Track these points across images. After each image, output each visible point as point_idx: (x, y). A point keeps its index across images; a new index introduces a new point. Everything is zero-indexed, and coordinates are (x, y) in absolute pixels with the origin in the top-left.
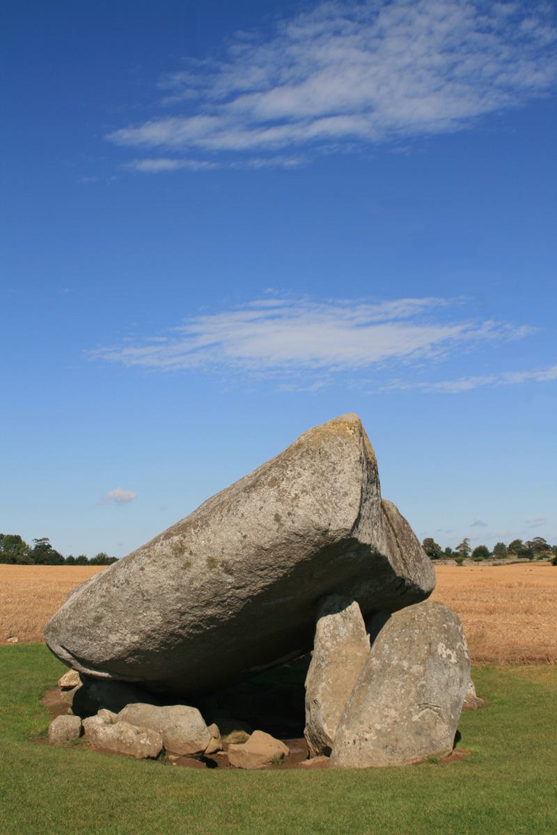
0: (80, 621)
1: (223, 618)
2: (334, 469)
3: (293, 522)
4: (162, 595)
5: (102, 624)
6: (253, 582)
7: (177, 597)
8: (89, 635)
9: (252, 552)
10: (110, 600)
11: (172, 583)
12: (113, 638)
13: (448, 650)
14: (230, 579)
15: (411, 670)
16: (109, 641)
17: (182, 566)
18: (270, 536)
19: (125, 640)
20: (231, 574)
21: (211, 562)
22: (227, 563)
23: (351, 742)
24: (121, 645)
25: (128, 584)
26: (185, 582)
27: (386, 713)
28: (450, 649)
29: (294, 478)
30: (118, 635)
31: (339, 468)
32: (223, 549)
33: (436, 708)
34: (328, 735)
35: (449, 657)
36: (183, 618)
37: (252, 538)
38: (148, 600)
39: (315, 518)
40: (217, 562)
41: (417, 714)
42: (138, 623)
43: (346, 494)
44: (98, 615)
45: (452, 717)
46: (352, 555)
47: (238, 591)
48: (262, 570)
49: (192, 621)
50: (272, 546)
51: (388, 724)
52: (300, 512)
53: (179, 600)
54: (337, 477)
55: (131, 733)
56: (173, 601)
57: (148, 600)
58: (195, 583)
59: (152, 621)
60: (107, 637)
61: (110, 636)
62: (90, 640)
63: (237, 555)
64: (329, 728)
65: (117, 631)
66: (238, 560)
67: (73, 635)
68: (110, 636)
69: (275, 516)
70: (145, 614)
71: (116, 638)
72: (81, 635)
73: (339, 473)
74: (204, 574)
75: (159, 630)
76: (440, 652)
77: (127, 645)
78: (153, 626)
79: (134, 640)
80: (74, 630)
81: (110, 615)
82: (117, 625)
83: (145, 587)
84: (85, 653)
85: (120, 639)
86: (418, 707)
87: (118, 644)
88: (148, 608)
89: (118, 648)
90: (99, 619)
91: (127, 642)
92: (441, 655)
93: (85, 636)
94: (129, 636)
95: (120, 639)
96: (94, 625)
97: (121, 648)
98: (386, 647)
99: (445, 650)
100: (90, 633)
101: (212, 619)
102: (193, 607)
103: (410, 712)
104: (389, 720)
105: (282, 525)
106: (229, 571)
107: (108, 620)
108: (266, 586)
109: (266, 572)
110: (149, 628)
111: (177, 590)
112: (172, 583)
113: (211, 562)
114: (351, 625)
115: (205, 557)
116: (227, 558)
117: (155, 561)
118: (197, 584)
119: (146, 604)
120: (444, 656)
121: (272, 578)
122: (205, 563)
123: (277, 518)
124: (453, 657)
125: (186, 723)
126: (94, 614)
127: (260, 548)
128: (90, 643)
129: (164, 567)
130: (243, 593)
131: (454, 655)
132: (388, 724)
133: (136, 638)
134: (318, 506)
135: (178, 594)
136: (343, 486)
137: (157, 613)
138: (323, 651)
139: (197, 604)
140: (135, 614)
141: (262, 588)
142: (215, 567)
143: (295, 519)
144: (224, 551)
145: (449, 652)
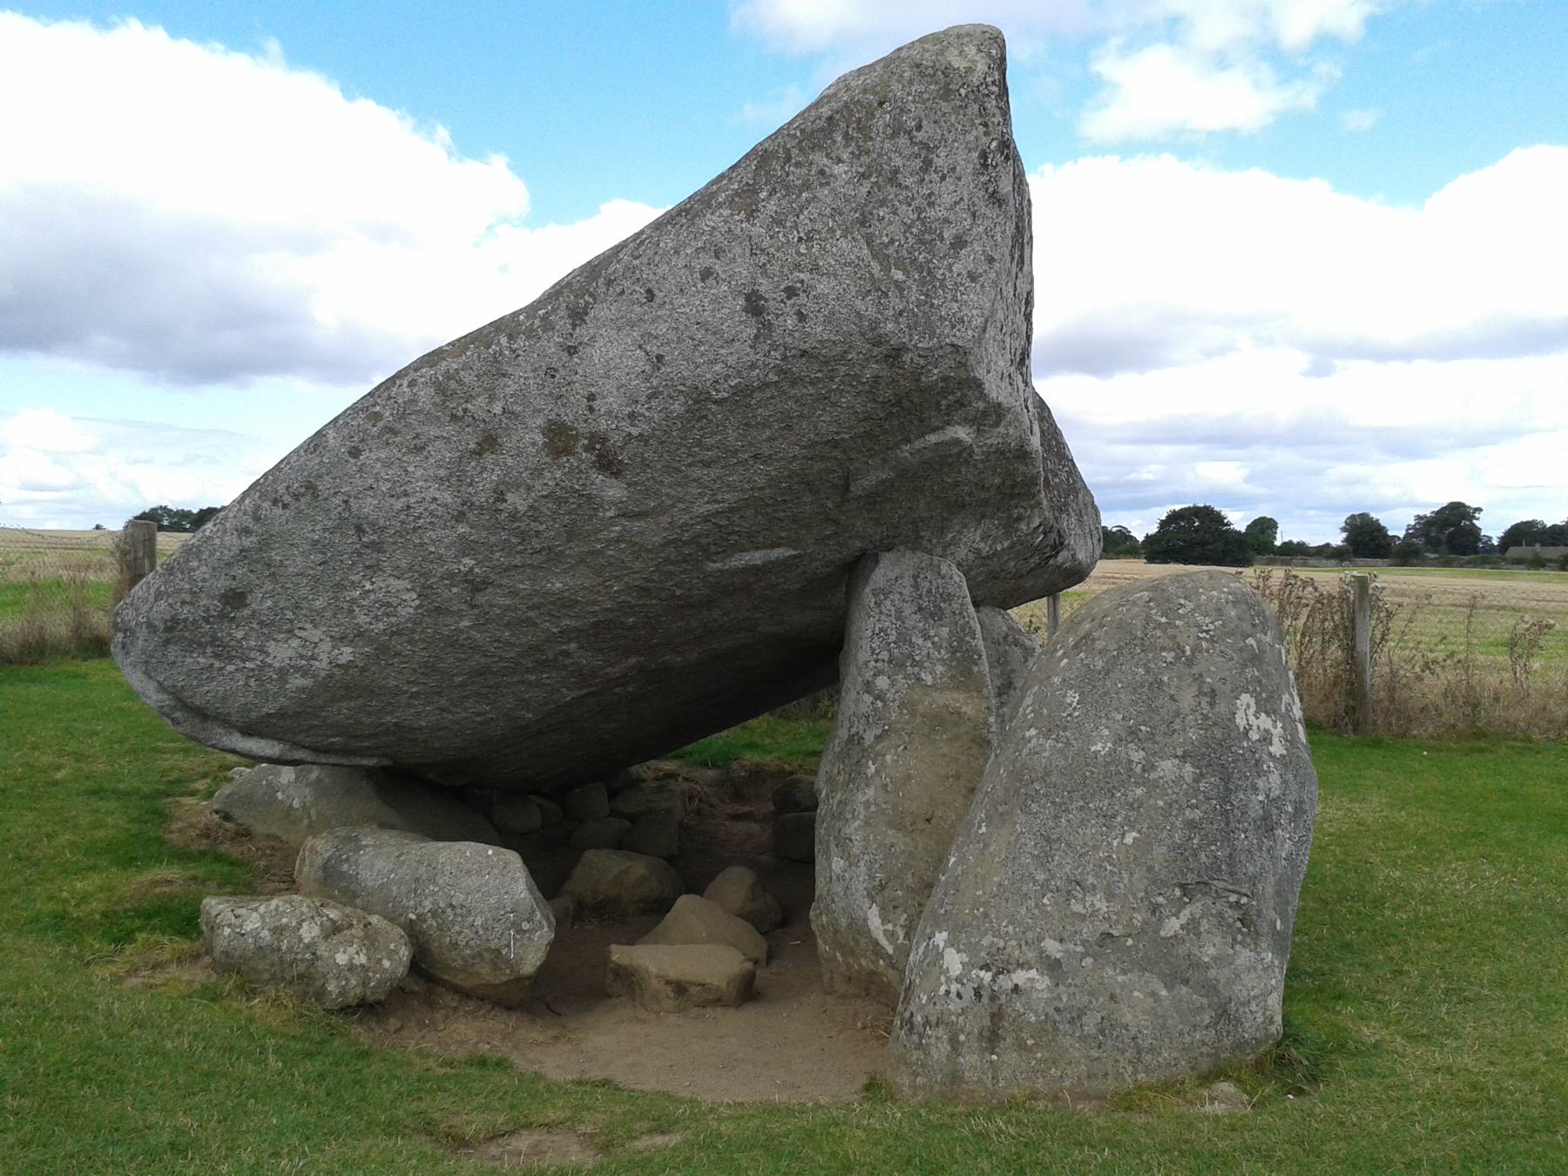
0: (183, 603)
1: (595, 603)
2: (928, 163)
3: (802, 317)
4: (414, 530)
5: (247, 612)
6: (680, 500)
7: (461, 537)
8: (212, 643)
9: (677, 408)
10: (264, 545)
11: (447, 497)
12: (282, 652)
14: (614, 491)
15: (1153, 776)
16: (269, 660)
17: (472, 446)
18: (731, 360)
19: (313, 658)
20: (617, 474)
21: (559, 438)
22: (605, 439)
23: (969, 993)
24: (305, 673)
25: (315, 496)
26: (482, 491)
27: (1077, 908)
29: (806, 186)
30: (295, 643)
31: (939, 162)
32: (592, 397)
33: (1233, 898)
34: (884, 942)
35: (1266, 739)
36: (480, 599)
37: (678, 368)
38: (377, 547)
39: (867, 307)
40: (576, 438)
41: (1177, 915)
42: (351, 611)
43: (959, 243)
44: (234, 584)
46: (963, 433)
47: (637, 525)
48: (706, 464)
49: (508, 608)
50: (736, 390)
51: (1084, 943)
52: (823, 286)
53: (466, 547)
54: (936, 188)
55: (309, 932)
56: (448, 548)
57: (377, 547)
58: (509, 496)
59: (389, 604)
60: (262, 651)
61: (271, 647)
62: (217, 656)
63: (632, 416)
64: (885, 920)
65: (290, 631)
66: (635, 432)
67: (167, 642)
68: (271, 647)
69: (748, 298)
70: (368, 587)
71: (290, 653)
72: (191, 642)
73: (943, 178)
74: (537, 472)
75: (413, 631)
76: (1240, 721)
77: (323, 674)
78: (393, 619)
79: (343, 660)
80: (168, 630)
81: (268, 587)
82: (289, 615)
83: (368, 506)
84: (207, 693)
85: (302, 657)
86: (1178, 892)
87: (298, 669)
88: (374, 569)
89: (297, 682)
90: (235, 598)
91: (322, 665)
93: (200, 644)
94: (326, 646)
95: (302, 657)
96: (222, 616)
97: (307, 682)
98: (1073, 697)
100: (214, 638)
101: (565, 603)
102: (507, 569)
103: (1154, 909)
104: (1088, 931)
105: (768, 326)
106: (608, 464)
107: (261, 603)
108: (717, 513)
109: (715, 472)
110: (381, 626)
111: (460, 517)
112: (447, 497)
113: (559, 438)
114: (945, 631)
115: (540, 421)
116: (603, 425)
117: (395, 433)
118: (516, 501)
119: (371, 557)
120: (1254, 736)
121: (735, 489)
122: (540, 439)
123: (755, 305)
124: (1275, 740)
125: (483, 889)
126: (223, 583)
127: (699, 399)
128: (217, 664)
129: (419, 449)
130: (652, 532)
131: (1277, 731)
132: (1084, 943)
133: (346, 654)
134: (876, 267)
135: (462, 529)
136: (952, 217)
137: (404, 584)
138: (868, 698)
139: (518, 561)
140: (340, 587)
142: (567, 451)
143: (810, 307)
144: (596, 404)
145: (1265, 722)
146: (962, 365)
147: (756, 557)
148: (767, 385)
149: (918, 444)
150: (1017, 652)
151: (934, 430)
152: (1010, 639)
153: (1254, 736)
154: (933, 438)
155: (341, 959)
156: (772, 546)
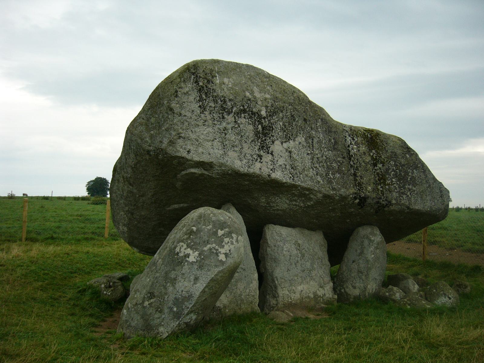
13: (189, 249)
28: (191, 249)
35: (188, 256)
41: (148, 301)
45: (175, 309)
76: (177, 250)
92: (178, 253)
99: (185, 249)
120: (181, 255)
141: (153, 196)
145: (189, 251)
146: (166, 153)
147: (176, 206)
148: (137, 163)
149: (181, 174)
150: (366, 242)
151: (183, 170)
152: (366, 237)
153: (181, 255)
154: (183, 173)
155: (105, 292)
156: (180, 203)
